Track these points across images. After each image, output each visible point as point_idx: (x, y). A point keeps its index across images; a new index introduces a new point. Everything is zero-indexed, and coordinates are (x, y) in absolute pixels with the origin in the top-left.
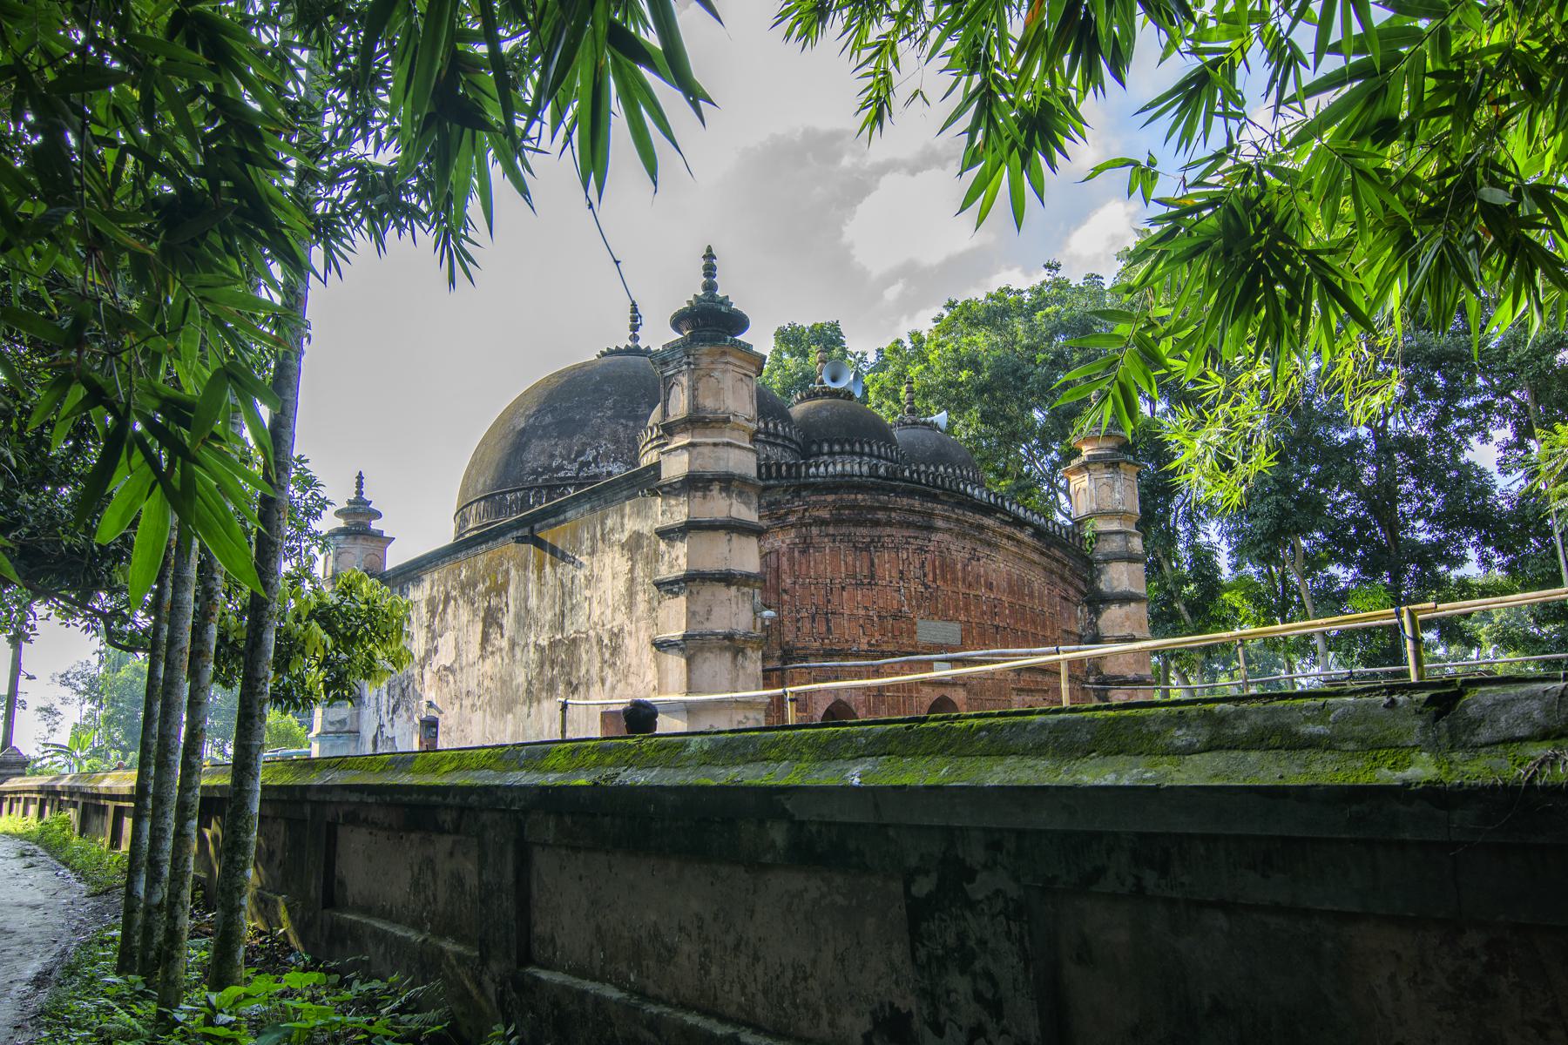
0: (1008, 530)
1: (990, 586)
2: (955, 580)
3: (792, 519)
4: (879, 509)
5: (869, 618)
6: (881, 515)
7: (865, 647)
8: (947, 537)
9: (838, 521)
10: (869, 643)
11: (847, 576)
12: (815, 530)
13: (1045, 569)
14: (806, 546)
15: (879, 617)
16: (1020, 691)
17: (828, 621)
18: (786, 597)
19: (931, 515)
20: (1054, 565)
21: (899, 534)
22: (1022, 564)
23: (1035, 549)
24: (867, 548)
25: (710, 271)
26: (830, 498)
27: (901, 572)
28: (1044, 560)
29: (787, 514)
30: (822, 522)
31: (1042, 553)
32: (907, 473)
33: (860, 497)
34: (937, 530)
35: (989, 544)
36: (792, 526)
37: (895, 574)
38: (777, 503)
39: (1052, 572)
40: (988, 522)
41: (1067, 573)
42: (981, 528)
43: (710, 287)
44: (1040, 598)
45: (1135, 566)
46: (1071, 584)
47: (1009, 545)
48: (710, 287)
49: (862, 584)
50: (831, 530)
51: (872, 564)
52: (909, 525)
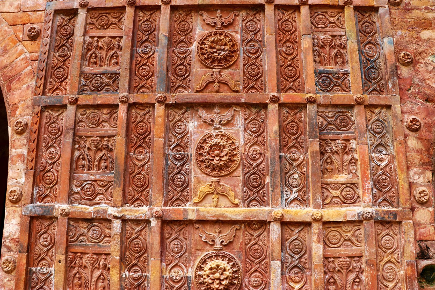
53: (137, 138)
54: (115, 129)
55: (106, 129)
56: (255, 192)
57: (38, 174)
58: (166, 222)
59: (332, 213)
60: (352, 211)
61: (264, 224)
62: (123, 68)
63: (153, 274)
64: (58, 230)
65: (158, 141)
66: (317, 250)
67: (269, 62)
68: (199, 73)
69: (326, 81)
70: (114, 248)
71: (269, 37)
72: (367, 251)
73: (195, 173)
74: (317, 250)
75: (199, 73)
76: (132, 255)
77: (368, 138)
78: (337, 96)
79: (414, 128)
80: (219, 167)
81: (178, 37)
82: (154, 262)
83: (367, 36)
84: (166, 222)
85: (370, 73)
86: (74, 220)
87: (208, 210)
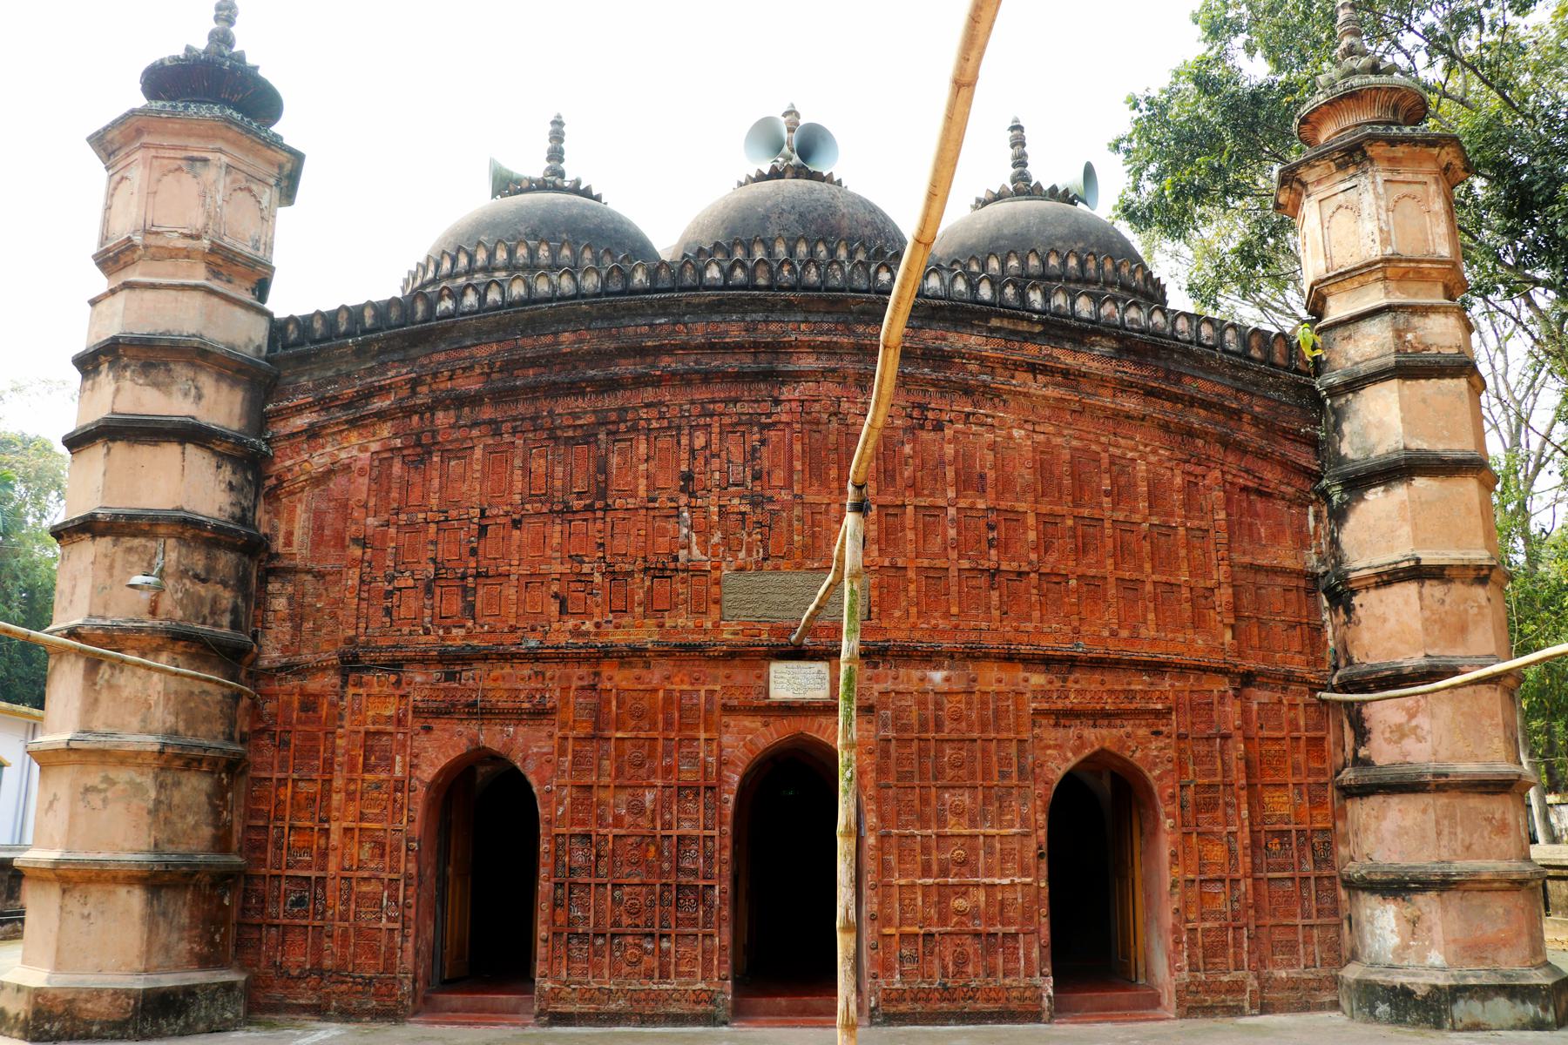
0: (1031, 351)
1: (969, 481)
3: (379, 404)
4: (623, 353)
5: (584, 579)
6: (625, 368)
7: (563, 639)
8: (830, 388)
9: (500, 396)
10: (576, 632)
11: (528, 498)
12: (442, 418)
13: (1165, 427)
14: (420, 451)
15: (612, 575)
16: (1064, 717)
17: (465, 590)
18: (358, 552)
19: (777, 348)
20: (1197, 417)
21: (677, 400)
22: (1085, 424)
23: (1125, 387)
24: (589, 438)
26: (482, 352)
27: (688, 477)
28: (1160, 410)
30: (460, 401)
31: (1150, 393)
33: (566, 337)
34: (797, 377)
35: (967, 391)
36: (382, 416)
37: (668, 481)
39: (1191, 433)
41: (1247, 433)
43: (222, 38)
44: (1154, 499)
45: (1428, 387)
46: (1264, 456)
47: (1038, 387)
48: (222, 38)
49: (568, 510)
50: (487, 413)
51: (603, 468)
52: (707, 377)
53: (925, 801)
54: (914, 797)
55: (910, 797)
56: (973, 823)
57: (882, 818)
58: (938, 836)
59: (1003, 832)
60: (1014, 830)
61: (977, 836)
62: (916, 770)
63: (934, 857)
64: (893, 841)
65: (934, 802)
66: (998, 846)
67: (978, 767)
68: (950, 773)
69: (1003, 775)
70: (918, 848)
71: (979, 755)
72: (1017, 846)
73: (949, 816)
74: (998, 846)
75: (950, 773)
76: (925, 850)
77: (1021, 801)
78: (1006, 782)
79: (1040, 796)
80: (959, 814)
81: (940, 754)
82: (934, 852)
83: (1021, 753)
84: (938, 836)
85: (1021, 771)
86: (901, 836)
87: (955, 831)
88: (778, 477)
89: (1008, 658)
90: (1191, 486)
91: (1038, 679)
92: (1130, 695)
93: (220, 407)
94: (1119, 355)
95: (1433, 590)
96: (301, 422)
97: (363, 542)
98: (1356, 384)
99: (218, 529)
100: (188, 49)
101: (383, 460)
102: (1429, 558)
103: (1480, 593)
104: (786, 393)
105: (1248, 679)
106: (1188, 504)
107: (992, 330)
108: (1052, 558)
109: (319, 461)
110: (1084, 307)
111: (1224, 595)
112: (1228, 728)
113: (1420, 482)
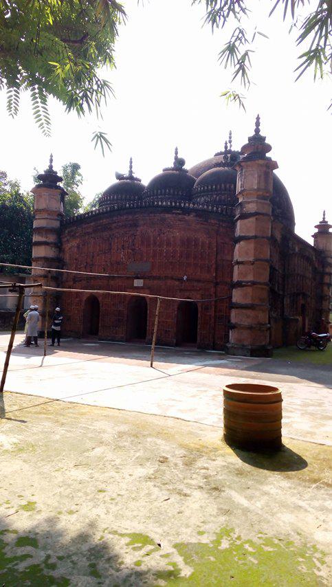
1: (168, 244)
2: (149, 245)
5: (107, 265)
9: (95, 231)
24: (108, 239)
25: (51, 161)
26: (92, 224)
27: (123, 246)
29: (75, 234)
30: (88, 233)
31: (202, 224)
32: (128, 205)
38: (72, 231)
40: (167, 215)
42: (163, 220)
43: (51, 167)
45: (246, 221)
48: (51, 167)
50: (93, 235)
51: (111, 244)
88: (137, 245)
89: (172, 278)
90: (210, 243)
91: (177, 283)
92: (193, 286)
93: (51, 238)
94: (196, 216)
95: (241, 266)
96: (66, 239)
97: (76, 259)
98: (238, 219)
99: (52, 259)
100: (45, 171)
101: (78, 247)
102: (240, 260)
103: (251, 267)
104: (138, 229)
105: (217, 284)
106: (209, 248)
107: (173, 213)
108: (183, 259)
109: (69, 245)
110: (191, 205)
111: (214, 266)
112: (212, 293)
113: (241, 243)
